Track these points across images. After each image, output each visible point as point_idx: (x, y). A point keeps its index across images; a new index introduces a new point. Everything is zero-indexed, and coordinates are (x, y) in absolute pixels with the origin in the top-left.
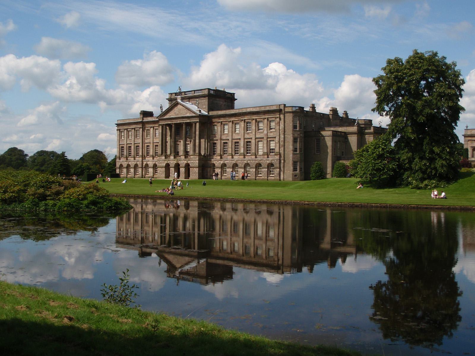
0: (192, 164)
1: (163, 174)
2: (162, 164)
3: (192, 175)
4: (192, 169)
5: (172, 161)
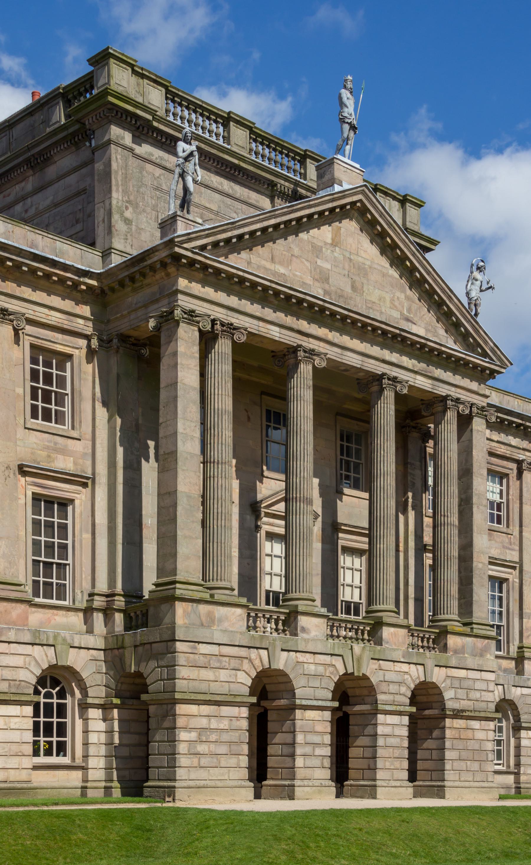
0: (461, 694)
1: (233, 761)
2: (223, 675)
3: (457, 765)
4: (459, 723)
5: (314, 661)
